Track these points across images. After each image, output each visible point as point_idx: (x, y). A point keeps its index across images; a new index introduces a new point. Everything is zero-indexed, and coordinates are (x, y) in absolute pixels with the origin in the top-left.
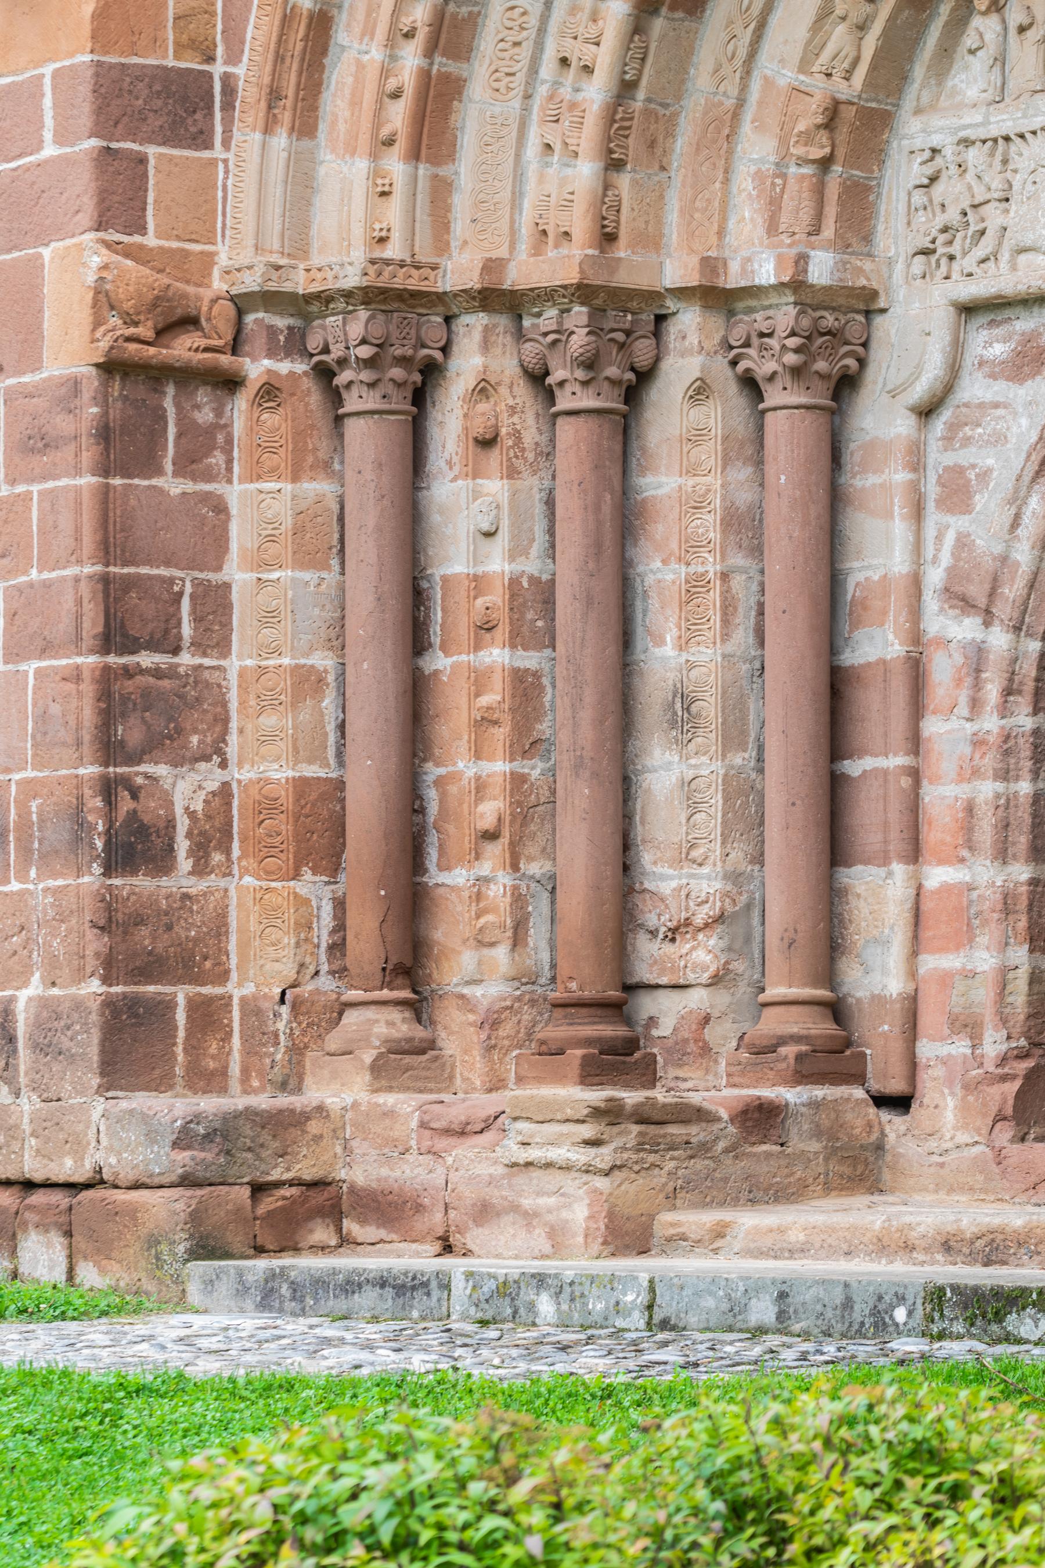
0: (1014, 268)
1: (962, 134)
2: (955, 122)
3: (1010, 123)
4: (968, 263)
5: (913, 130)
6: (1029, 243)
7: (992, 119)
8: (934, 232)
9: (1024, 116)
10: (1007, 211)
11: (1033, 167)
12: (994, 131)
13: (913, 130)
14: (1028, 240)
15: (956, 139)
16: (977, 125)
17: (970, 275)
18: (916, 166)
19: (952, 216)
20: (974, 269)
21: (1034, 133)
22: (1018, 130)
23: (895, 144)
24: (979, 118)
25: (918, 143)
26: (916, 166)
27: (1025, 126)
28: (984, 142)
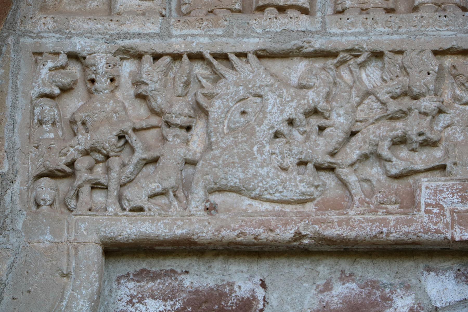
0: (211, 209)
1: (122, 43)
2: (114, 28)
3: (207, 40)
4: (137, 195)
5: (40, 27)
6: (233, 181)
7: (174, 32)
8: (72, 153)
9: (228, 34)
10: (187, 142)
11: (242, 92)
12: (178, 45)
13: (40, 27)
14: (235, 177)
15: (113, 47)
16: (149, 35)
17: (141, 209)
18: (44, 71)
19: (106, 137)
20: (146, 205)
21: (242, 55)
22: (218, 49)
23: (10, 41)
24: (152, 27)
25: (50, 43)
26: (44, 71)
27: (230, 46)
28: (156, 57)
